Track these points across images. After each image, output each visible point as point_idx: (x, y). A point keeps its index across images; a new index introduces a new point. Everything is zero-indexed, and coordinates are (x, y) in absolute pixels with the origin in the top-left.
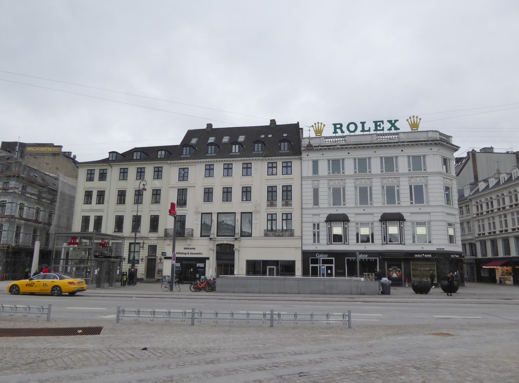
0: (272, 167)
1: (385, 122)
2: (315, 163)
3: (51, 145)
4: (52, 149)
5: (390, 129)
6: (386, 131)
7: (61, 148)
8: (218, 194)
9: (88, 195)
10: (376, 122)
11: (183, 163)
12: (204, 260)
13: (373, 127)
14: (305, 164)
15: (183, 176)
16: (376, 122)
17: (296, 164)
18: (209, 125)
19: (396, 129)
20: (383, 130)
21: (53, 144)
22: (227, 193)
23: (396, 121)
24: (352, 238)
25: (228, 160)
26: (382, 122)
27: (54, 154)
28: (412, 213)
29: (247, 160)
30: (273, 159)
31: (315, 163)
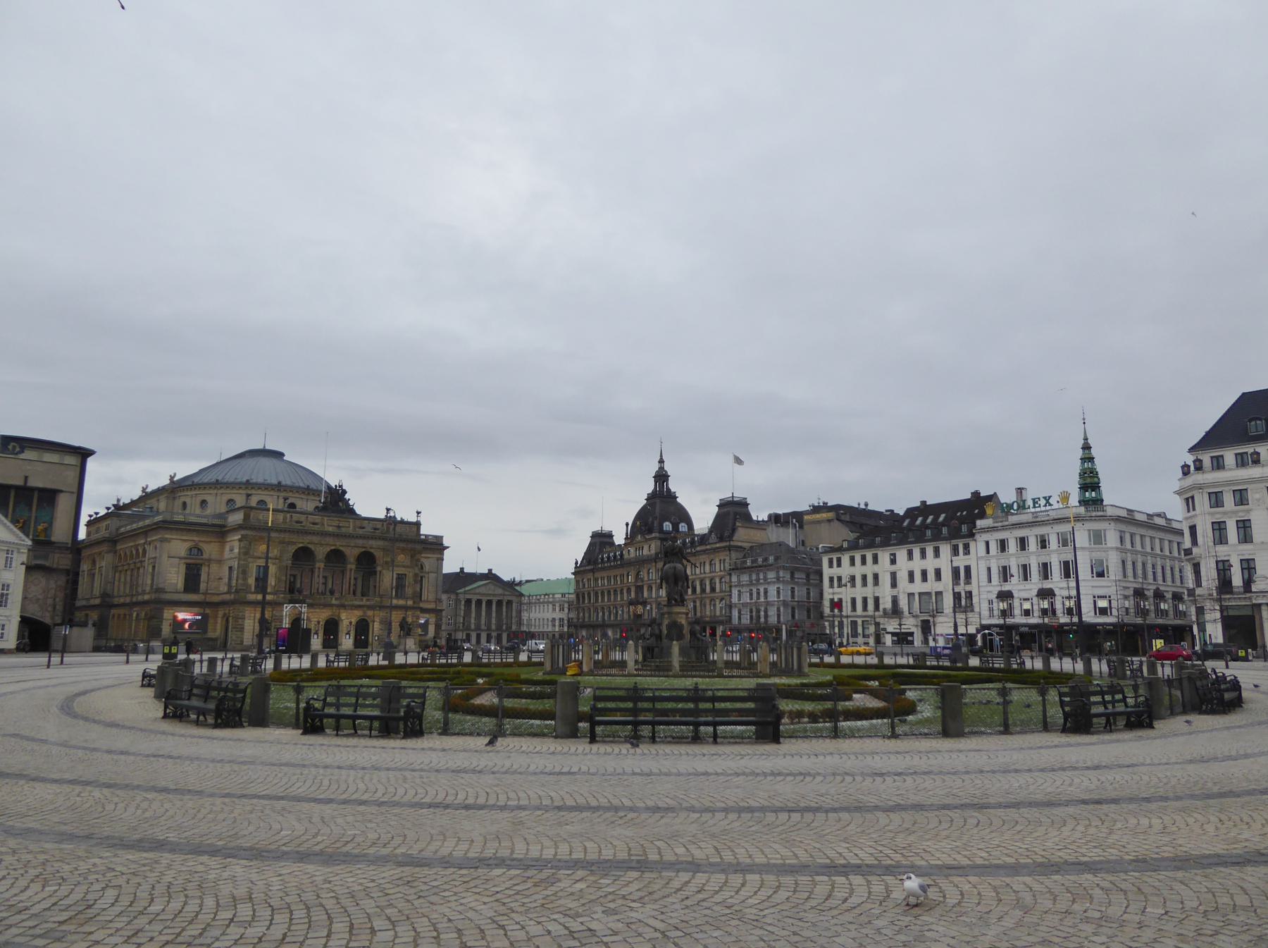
0: (955, 551)
1: (1042, 499)
2: (987, 543)
5: (1045, 506)
6: (1043, 509)
8: (918, 576)
9: (831, 579)
10: (1034, 500)
11: (892, 549)
12: (912, 634)
13: (1032, 506)
14: (978, 543)
15: (893, 562)
16: (1034, 500)
17: (972, 545)
18: (924, 503)
19: (1050, 505)
20: (1040, 506)
22: (924, 574)
23: (1050, 497)
24: (1017, 611)
25: (922, 545)
26: (1039, 499)
28: (1093, 587)
29: (936, 544)
30: (954, 542)
31: (987, 543)
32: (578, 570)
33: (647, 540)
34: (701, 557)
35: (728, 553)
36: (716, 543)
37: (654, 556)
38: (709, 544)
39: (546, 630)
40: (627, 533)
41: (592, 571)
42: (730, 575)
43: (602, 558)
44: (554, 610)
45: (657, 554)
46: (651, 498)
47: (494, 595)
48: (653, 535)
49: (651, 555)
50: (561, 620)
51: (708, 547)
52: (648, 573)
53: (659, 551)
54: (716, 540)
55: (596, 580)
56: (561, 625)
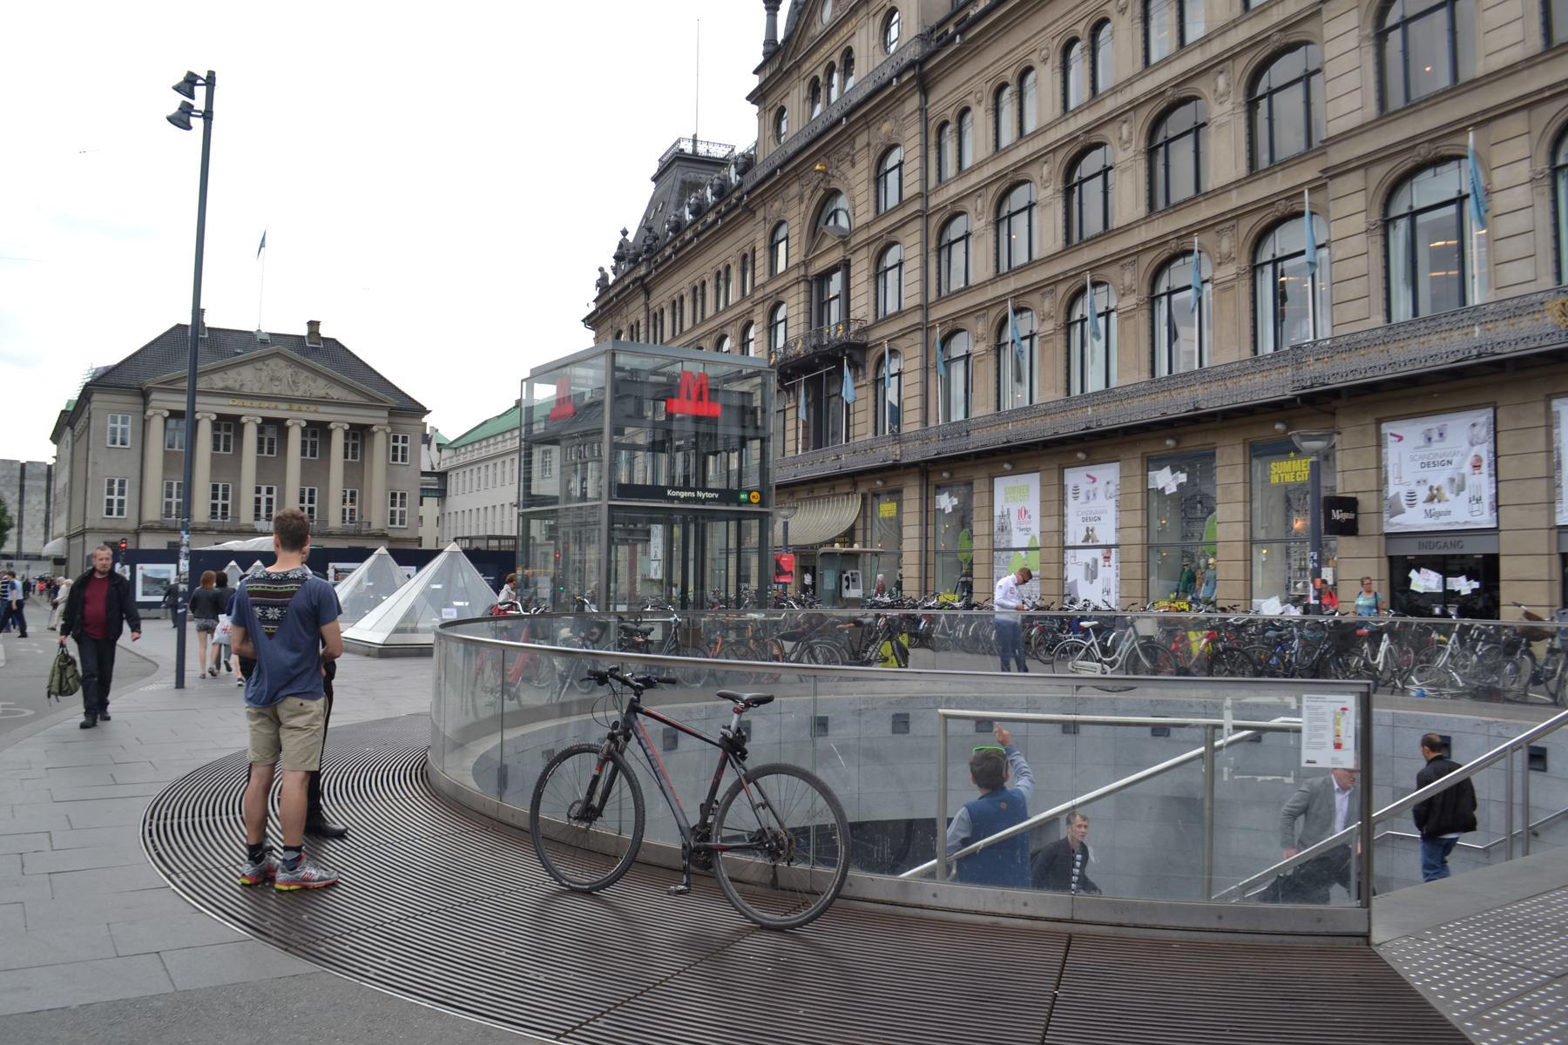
40: (770, 40)
52: (879, 178)
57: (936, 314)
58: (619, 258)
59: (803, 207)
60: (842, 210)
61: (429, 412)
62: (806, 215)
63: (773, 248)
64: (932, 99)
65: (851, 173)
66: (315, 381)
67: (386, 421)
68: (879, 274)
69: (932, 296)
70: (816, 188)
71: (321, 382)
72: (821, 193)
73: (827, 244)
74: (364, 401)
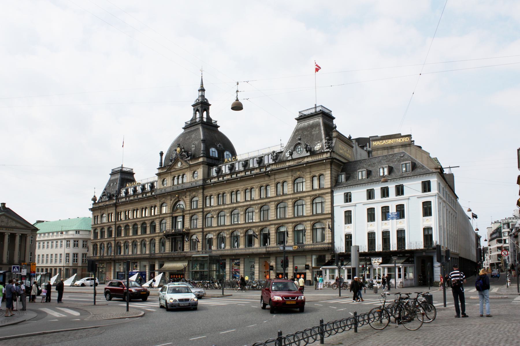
3: (398, 136)
4: (401, 140)
7: (410, 137)
21: (400, 134)
27: (404, 145)
32: (97, 206)
33: (191, 166)
34: (277, 176)
35: (329, 166)
36: (307, 157)
37: (201, 183)
38: (293, 160)
39: (58, 264)
40: (161, 163)
41: (116, 205)
42: (332, 192)
43: (127, 193)
44: (68, 245)
45: (204, 180)
46: (190, 126)
47: (7, 228)
48: (201, 160)
49: (196, 181)
50: (68, 255)
51: (291, 163)
53: (206, 177)
54: (305, 154)
55: (117, 214)
56: (67, 261)
57: (205, 230)
58: (104, 194)
59: (172, 202)
60: (182, 205)
61: (39, 230)
62: (172, 204)
63: (161, 206)
64: (205, 191)
65: (185, 199)
66: (13, 222)
67: (30, 233)
68: (191, 220)
69: (204, 227)
70: (176, 199)
71: (14, 222)
72: (177, 200)
73: (179, 211)
74: (22, 226)
